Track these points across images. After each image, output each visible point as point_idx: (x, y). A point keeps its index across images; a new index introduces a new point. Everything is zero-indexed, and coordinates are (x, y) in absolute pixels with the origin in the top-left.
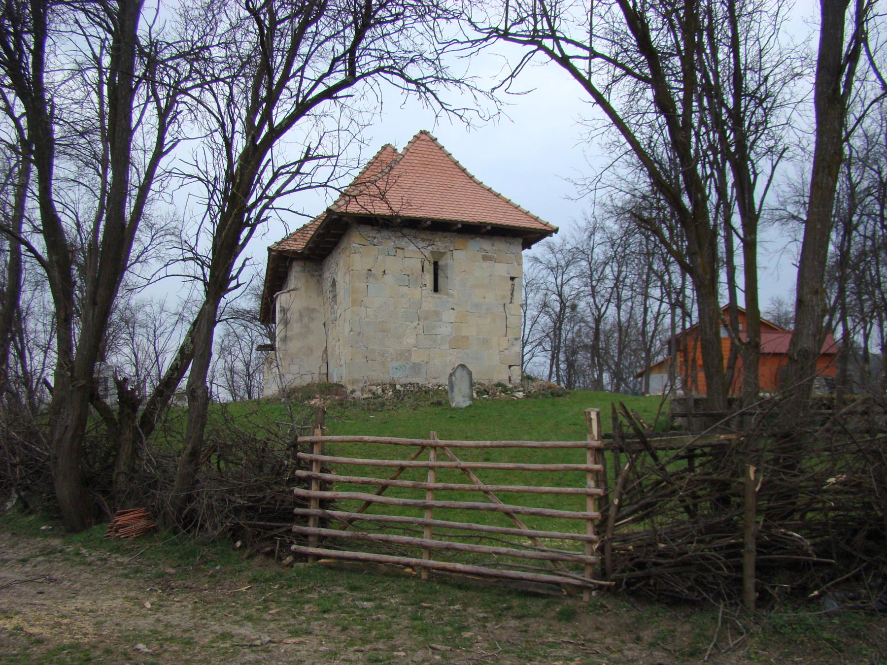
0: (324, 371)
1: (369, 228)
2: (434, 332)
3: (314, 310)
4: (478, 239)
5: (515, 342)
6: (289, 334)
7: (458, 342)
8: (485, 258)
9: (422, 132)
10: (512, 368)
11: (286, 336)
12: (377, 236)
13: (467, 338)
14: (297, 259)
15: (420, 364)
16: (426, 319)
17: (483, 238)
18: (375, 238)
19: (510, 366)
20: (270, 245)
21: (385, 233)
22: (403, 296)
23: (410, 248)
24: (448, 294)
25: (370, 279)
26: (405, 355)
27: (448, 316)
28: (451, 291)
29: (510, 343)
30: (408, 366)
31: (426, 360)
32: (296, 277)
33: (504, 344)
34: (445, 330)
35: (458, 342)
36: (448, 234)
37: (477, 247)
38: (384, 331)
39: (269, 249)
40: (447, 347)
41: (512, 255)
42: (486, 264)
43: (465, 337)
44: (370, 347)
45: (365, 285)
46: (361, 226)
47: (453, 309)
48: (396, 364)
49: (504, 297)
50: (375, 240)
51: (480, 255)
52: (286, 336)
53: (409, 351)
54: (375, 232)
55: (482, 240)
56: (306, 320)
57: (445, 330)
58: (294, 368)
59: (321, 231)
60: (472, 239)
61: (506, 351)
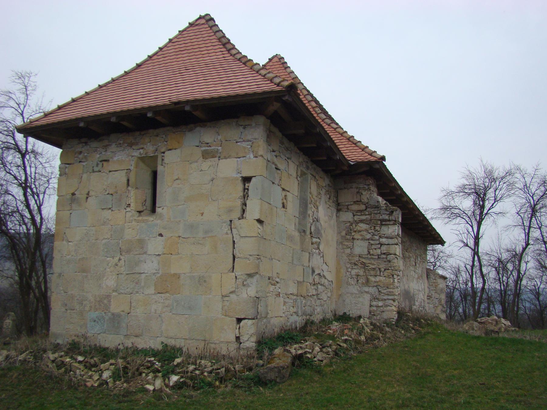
2: (137, 270)
4: (198, 129)
5: (249, 281)
7: (167, 283)
8: (206, 155)
9: (201, 18)
10: (243, 322)
13: (177, 276)
15: (119, 316)
16: (128, 251)
17: (205, 126)
18: (81, 153)
19: (239, 320)
21: (94, 144)
22: (104, 223)
23: (115, 159)
25: (74, 206)
26: (103, 302)
27: (155, 246)
29: (239, 281)
30: (107, 318)
31: (127, 310)
33: (229, 283)
34: (150, 266)
35: (167, 283)
37: (193, 141)
38: (84, 271)
40: (152, 290)
41: (244, 144)
42: (206, 164)
43: (175, 275)
44: (70, 293)
45: (69, 212)
47: (161, 235)
48: (94, 315)
49: (230, 210)
51: (198, 152)
53: (108, 297)
54: (81, 145)
57: (150, 266)
60: (191, 130)
61: (233, 296)
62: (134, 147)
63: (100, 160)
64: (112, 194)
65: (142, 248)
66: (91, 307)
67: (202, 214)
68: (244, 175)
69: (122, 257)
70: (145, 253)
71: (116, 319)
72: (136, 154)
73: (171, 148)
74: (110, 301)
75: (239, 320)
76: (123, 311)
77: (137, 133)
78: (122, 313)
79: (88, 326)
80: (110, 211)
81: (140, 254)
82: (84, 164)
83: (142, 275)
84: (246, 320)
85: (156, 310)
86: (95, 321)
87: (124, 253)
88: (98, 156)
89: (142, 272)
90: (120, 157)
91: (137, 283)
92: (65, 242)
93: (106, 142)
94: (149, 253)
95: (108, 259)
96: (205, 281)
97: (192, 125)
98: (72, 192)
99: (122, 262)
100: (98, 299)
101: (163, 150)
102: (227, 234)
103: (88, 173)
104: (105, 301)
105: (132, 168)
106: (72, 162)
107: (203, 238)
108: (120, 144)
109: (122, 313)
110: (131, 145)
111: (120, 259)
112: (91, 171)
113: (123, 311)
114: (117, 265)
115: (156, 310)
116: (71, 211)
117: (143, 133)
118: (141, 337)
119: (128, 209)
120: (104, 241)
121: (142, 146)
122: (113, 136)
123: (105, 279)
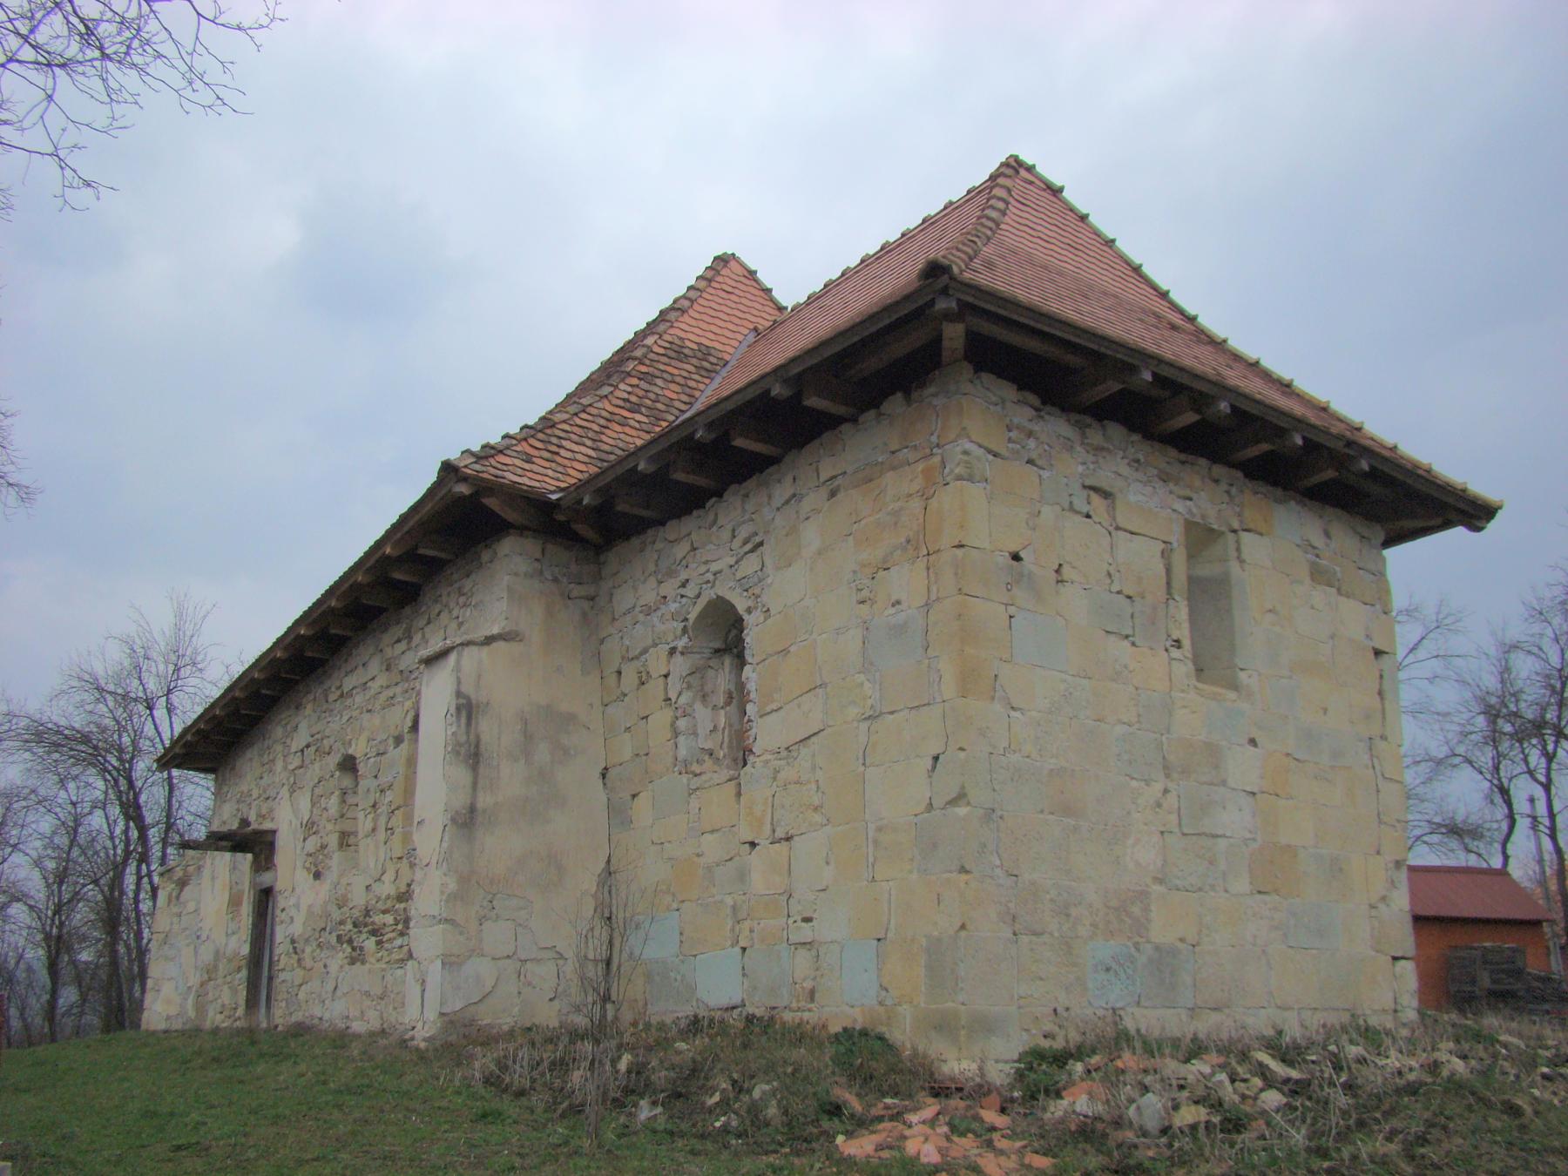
0: (596, 949)
1: (1009, 391)
3: (571, 718)
4: (1293, 503)
6: (484, 800)
11: (472, 809)
12: (1036, 427)
14: (522, 530)
18: (1030, 434)
19: (1395, 959)
20: (453, 455)
21: (1057, 427)
24: (1234, 686)
27: (1243, 767)
28: (1243, 676)
32: (504, 591)
36: (1218, 470)
39: (448, 468)
40: (1241, 885)
42: (1320, 596)
46: (986, 377)
47: (1253, 742)
50: (1032, 443)
52: (472, 809)
53: (1143, 895)
55: (1298, 508)
56: (542, 753)
58: (497, 936)
59: (777, 390)
60: (1279, 501)
62: (1171, 485)
63: (1088, 483)
64: (1129, 597)
65: (1217, 767)
66: (1094, 925)
67: (1325, 711)
68: (1378, 646)
69: (1171, 786)
70: (1224, 783)
71: (1165, 961)
72: (1180, 506)
73: (1251, 526)
74: (1146, 909)
75: (1395, 959)
76: (1182, 940)
77: (1173, 452)
78: (1180, 945)
79: (1090, 985)
80: (1126, 643)
81: (1212, 784)
82: (1045, 474)
83: (1220, 840)
84: (1403, 962)
85: (1255, 937)
86: (1108, 970)
87: (1175, 775)
88: (1080, 468)
89: (1220, 832)
90: (1141, 498)
91: (1211, 863)
92: (997, 707)
93: (1095, 437)
94: (1231, 783)
95: (1134, 783)
96: (1341, 870)
97: (1279, 492)
98: (1014, 548)
99: (1171, 800)
100: (1114, 903)
101: (1236, 525)
102: (1367, 767)
103: (1058, 508)
104: (1136, 910)
105: (1173, 539)
106: (1003, 452)
107: (1333, 767)
108: (1138, 461)
109: (1180, 945)
110: (1165, 478)
111: (1166, 791)
112: (1066, 506)
113: (1182, 940)
114: (1159, 805)
115: (1255, 937)
116: (1012, 610)
117: (1183, 457)
118: (1226, 1011)
119: (1175, 653)
120: (1119, 729)
121: (1188, 493)
122: (1116, 430)
123: (1130, 842)
